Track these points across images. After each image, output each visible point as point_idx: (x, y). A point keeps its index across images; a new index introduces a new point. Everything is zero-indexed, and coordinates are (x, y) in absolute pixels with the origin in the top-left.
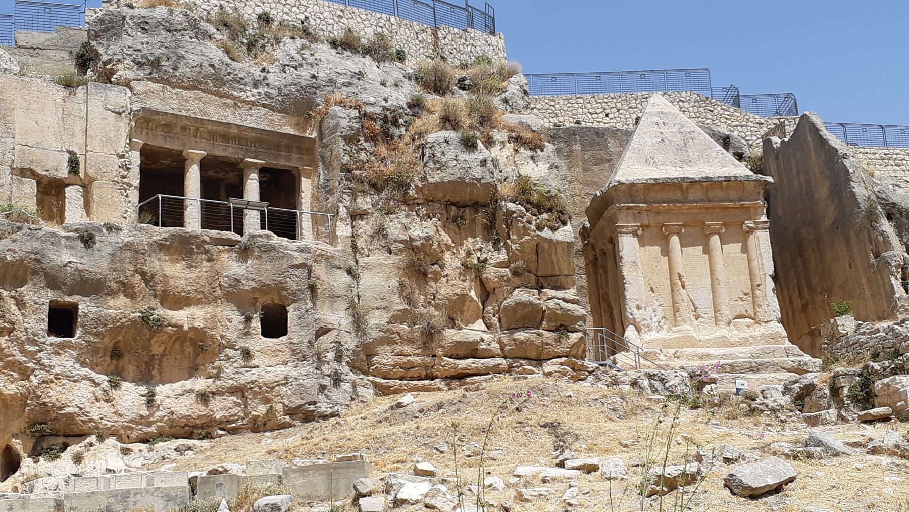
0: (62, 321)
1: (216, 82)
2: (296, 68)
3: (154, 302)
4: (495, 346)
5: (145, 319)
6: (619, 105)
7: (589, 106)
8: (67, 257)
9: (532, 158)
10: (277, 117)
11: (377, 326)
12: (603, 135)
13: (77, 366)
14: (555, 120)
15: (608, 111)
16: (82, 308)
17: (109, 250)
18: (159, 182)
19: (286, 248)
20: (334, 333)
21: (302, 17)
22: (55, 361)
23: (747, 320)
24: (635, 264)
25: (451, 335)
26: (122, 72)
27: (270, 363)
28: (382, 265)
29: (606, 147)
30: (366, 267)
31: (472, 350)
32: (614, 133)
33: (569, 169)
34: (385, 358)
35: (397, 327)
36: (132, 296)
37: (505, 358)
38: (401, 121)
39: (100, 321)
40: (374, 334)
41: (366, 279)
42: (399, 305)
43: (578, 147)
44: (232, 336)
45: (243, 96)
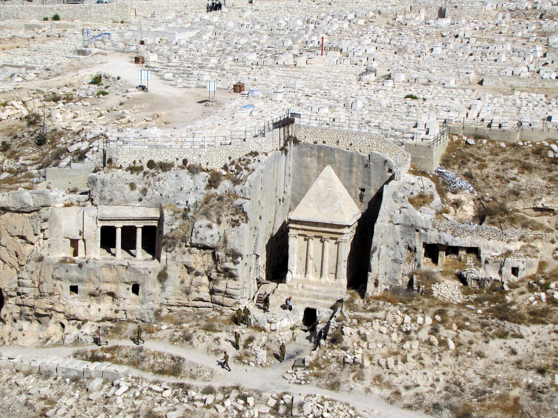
0: (74, 289)
2: (156, 190)
4: (210, 300)
5: (97, 289)
6: (344, 136)
7: (331, 134)
8: (74, 273)
10: (148, 209)
11: (170, 291)
13: (79, 302)
14: (315, 139)
16: (79, 287)
18: (107, 238)
19: (140, 269)
20: (153, 295)
22: (72, 302)
24: (293, 249)
25: (194, 295)
29: (334, 157)
32: (338, 150)
33: (318, 164)
36: (94, 283)
37: (212, 303)
39: (83, 291)
43: (322, 155)
45: (136, 205)
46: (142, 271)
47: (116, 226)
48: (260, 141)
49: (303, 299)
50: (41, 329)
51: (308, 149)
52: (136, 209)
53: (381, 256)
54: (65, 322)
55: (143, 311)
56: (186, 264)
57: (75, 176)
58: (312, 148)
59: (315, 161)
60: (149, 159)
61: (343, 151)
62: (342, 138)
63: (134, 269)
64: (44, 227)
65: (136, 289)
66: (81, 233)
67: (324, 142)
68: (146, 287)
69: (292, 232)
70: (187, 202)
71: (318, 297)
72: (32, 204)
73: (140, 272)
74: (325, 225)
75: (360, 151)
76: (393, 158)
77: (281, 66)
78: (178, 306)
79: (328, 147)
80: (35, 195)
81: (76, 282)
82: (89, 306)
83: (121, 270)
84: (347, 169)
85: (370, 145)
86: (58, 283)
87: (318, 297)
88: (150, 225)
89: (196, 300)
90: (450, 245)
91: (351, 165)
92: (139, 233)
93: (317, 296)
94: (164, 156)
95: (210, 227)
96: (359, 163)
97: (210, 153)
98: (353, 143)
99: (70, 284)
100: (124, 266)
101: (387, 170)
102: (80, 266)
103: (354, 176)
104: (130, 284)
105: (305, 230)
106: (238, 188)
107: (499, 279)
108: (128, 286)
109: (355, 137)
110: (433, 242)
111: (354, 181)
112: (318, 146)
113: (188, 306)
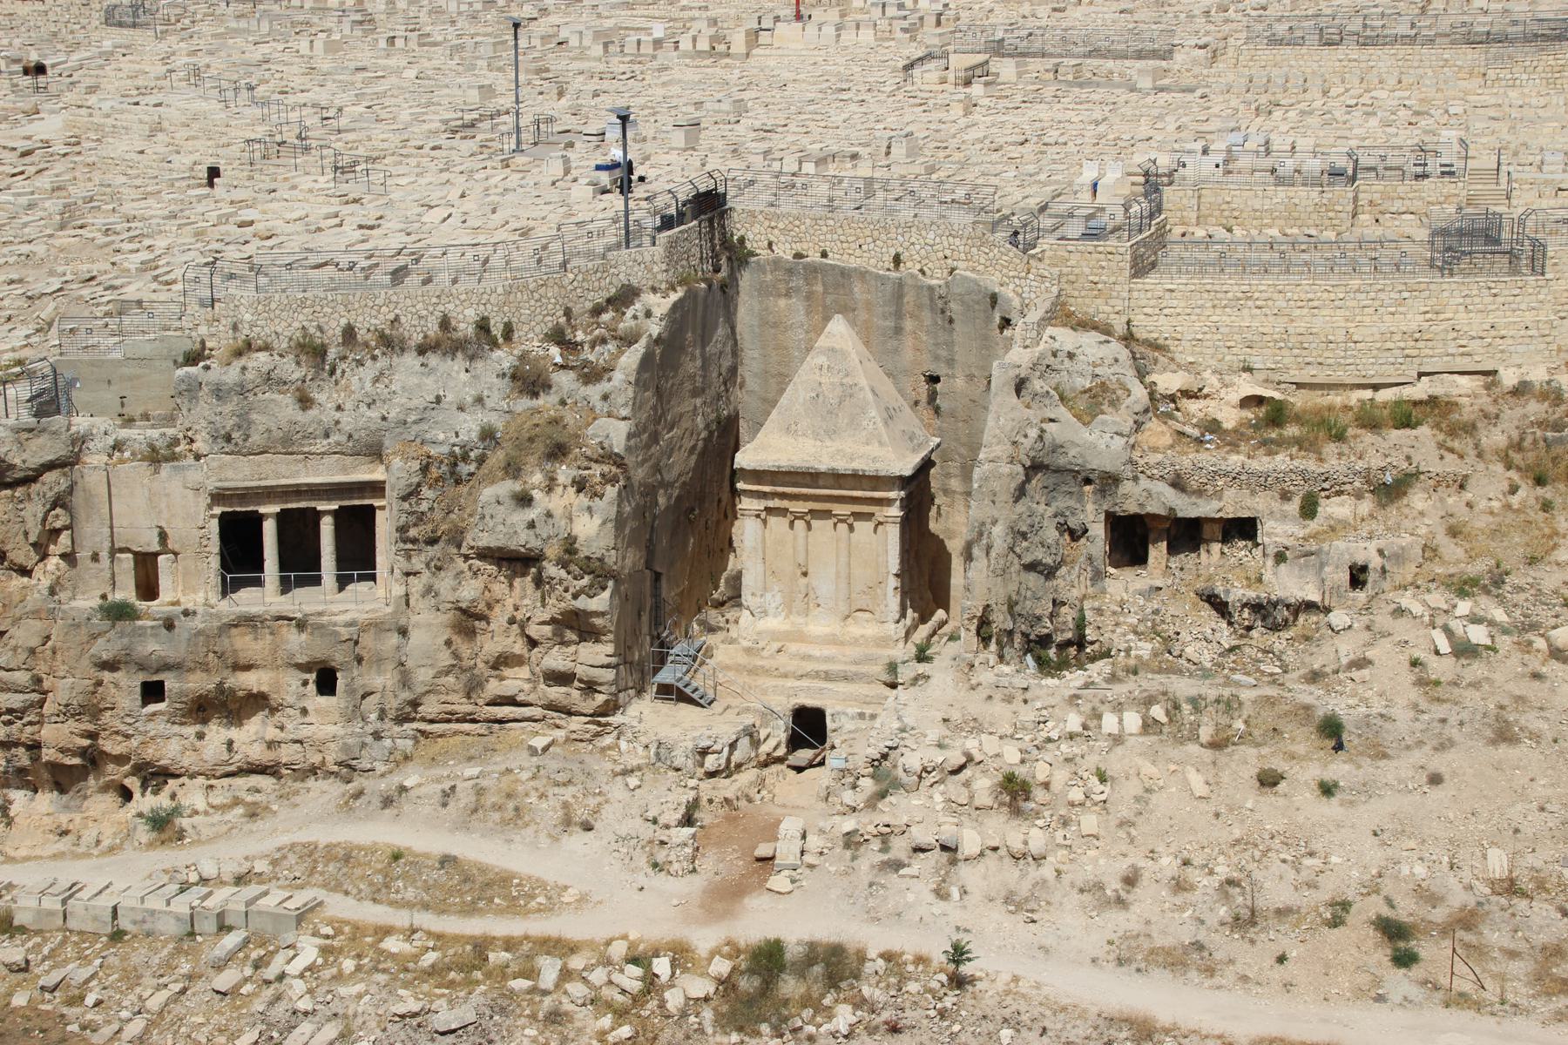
0: (152, 692)
1: (288, 443)
2: (369, 406)
3: (226, 673)
6: (876, 233)
7: (840, 231)
8: (154, 647)
9: (589, 509)
12: (850, 277)
14: (798, 247)
15: (861, 241)
17: (186, 635)
19: (335, 625)
20: (378, 695)
21: (391, 316)
22: (150, 726)
23: (867, 615)
25: (494, 688)
26: (200, 446)
27: (323, 722)
28: (430, 625)
29: (851, 291)
30: (417, 625)
31: (511, 701)
32: (863, 274)
33: (808, 313)
34: (430, 707)
35: (443, 680)
38: (472, 454)
39: (181, 693)
40: (420, 689)
41: (416, 637)
42: (445, 659)
43: (819, 288)
44: (290, 699)
46: (343, 630)
47: (262, 510)
48: (648, 258)
49: (790, 683)
50: (67, 807)
51: (780, 274)
52: (313, 462)
53: (993, 554)
54: (133, 783)
55: (350, 741)
56: (464, 605)
57: (138, 377)
58: (790, 271)
59: (797, 303)
60: (343, 322)
61: (878, 276)
62: (869, 240)
63: (322, 626)
64: (58, 524)
65: (326, 682)
66: (163, 536)
67: (824, 255)
68: (356, 673)
69: (746, 504)
70: (457, 435)
71: (828, 677)
72: (17, 461)
73: (336, 633)
74: (837, 478)
75: (922, 271)
76: (1011, 286)
77: (685, 55)
78: (449, 721)
79: (833, 267)
80: (25, 435)
81: (157, 671)
82: (200, 736)
83: (285, 629)
84: (890, 323)
85: (948, 253)
86: (107, 676)
87: (828, 677)
88: (357, 502)
89: (494, 703)
90: (1180, 515)
91: (899, 315)
92: (327, 527)
93: (826, 672)
94: (384, 309)
95: (524, 500)
96: (920, 307)
97: (512, 297)
98: (900, 250)
99: (142, 677)
100: (290, 619)
101: (998, 320)
102: (169, 625)
103: (909, 342)
104: (309, 671)
105: (783, 496)
106: (594, 392)
107: (1315, 597)
108: (307, 676)
109: (907, 236)
110: (1132, 508)
111: (908, 355)
112: (806, 267)
113: (474, 721)
